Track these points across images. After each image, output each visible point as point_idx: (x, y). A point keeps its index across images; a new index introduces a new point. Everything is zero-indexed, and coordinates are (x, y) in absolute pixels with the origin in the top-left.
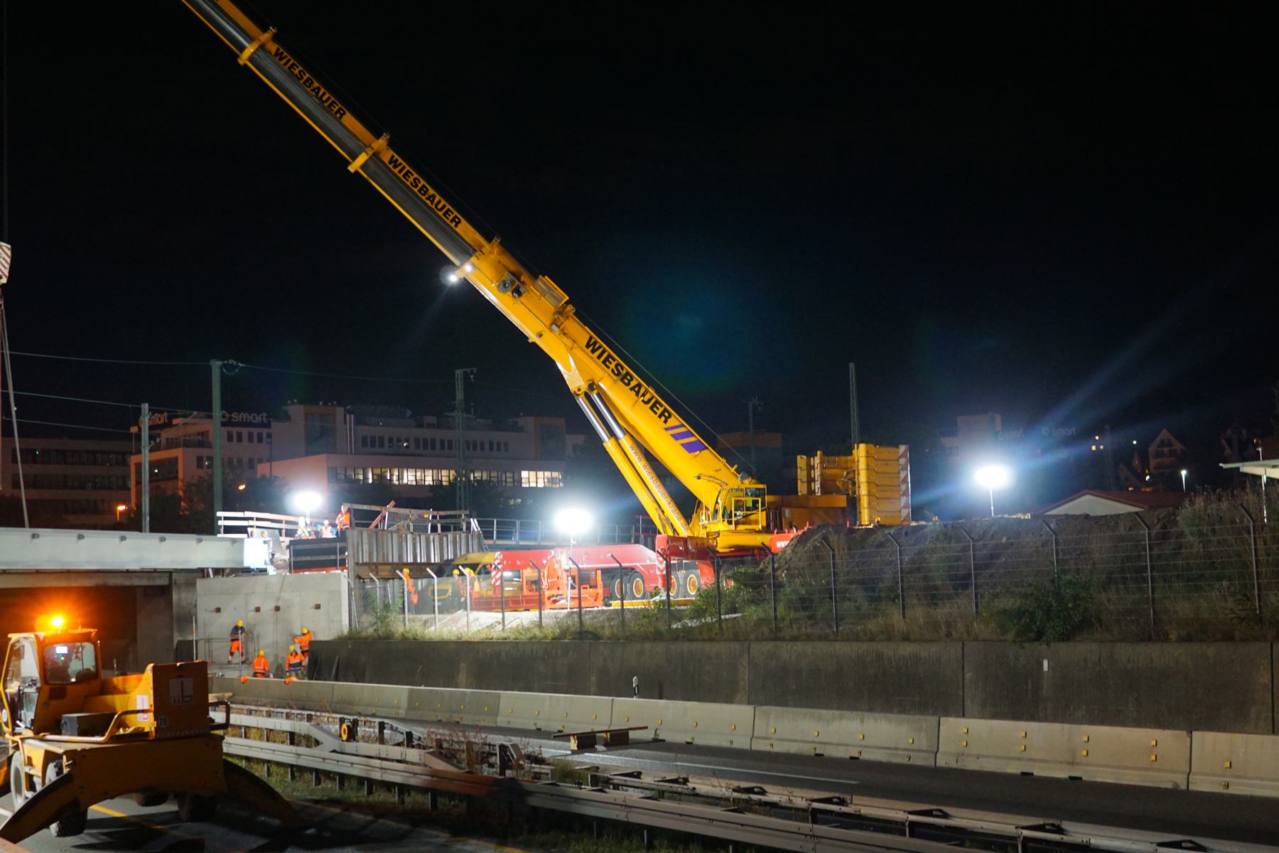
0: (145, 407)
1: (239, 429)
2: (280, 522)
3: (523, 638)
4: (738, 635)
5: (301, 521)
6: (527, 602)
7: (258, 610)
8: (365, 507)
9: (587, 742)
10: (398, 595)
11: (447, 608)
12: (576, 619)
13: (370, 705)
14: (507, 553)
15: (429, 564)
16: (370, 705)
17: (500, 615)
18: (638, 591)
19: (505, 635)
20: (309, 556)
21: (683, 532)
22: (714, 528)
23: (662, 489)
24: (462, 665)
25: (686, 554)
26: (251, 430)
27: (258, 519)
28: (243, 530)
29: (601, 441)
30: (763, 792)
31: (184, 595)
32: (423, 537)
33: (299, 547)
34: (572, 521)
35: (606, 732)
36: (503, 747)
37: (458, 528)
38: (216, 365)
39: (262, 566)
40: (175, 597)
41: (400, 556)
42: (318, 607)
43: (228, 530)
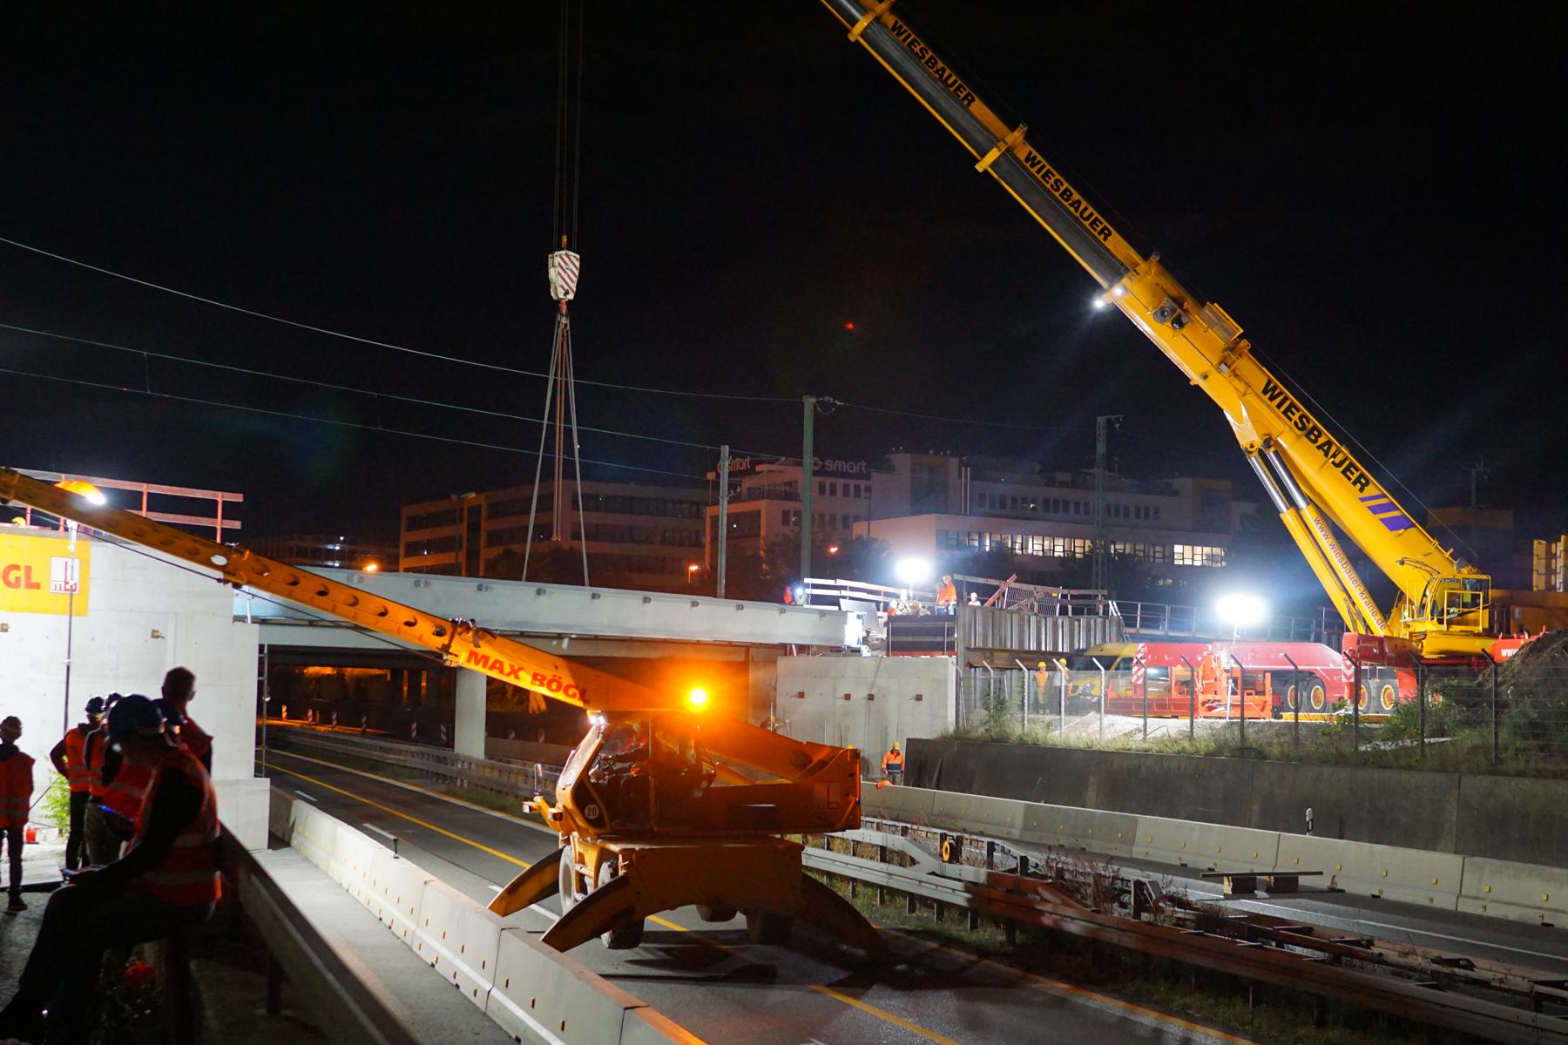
0: (725, 449)
1: (833, 480)
3: (1169, 751)
4: (1445, 764)
5: (903, 594)
6: (1177, 706)
7: (848, 697)
8: (981, 581)
9: (1244, 885)
10: (1016, 689)
13: (977, 821)
14: (1153, 645)
16: (977, 821)
17: (1141, 721)
19: (1146, 746)
20: (911, 637)
21: (1379, 631)
22: (1419, 627)
23: (1354, 575)
24: (1092, 779)
25: (1381, 658)
26: (847, 481)
27: (852, 589)
28: (835, 601)
29: (1277, 511)
30: (1470, 966)
32: (1050, 620)
33: (898, 624)
34: (1238, 611)
35: (1269, 874)
36: (1139, 884)
37: (1092, 611)
38: (809, 402)
39: (854, 645)
41: (1021, 642)
42: (919, 698)
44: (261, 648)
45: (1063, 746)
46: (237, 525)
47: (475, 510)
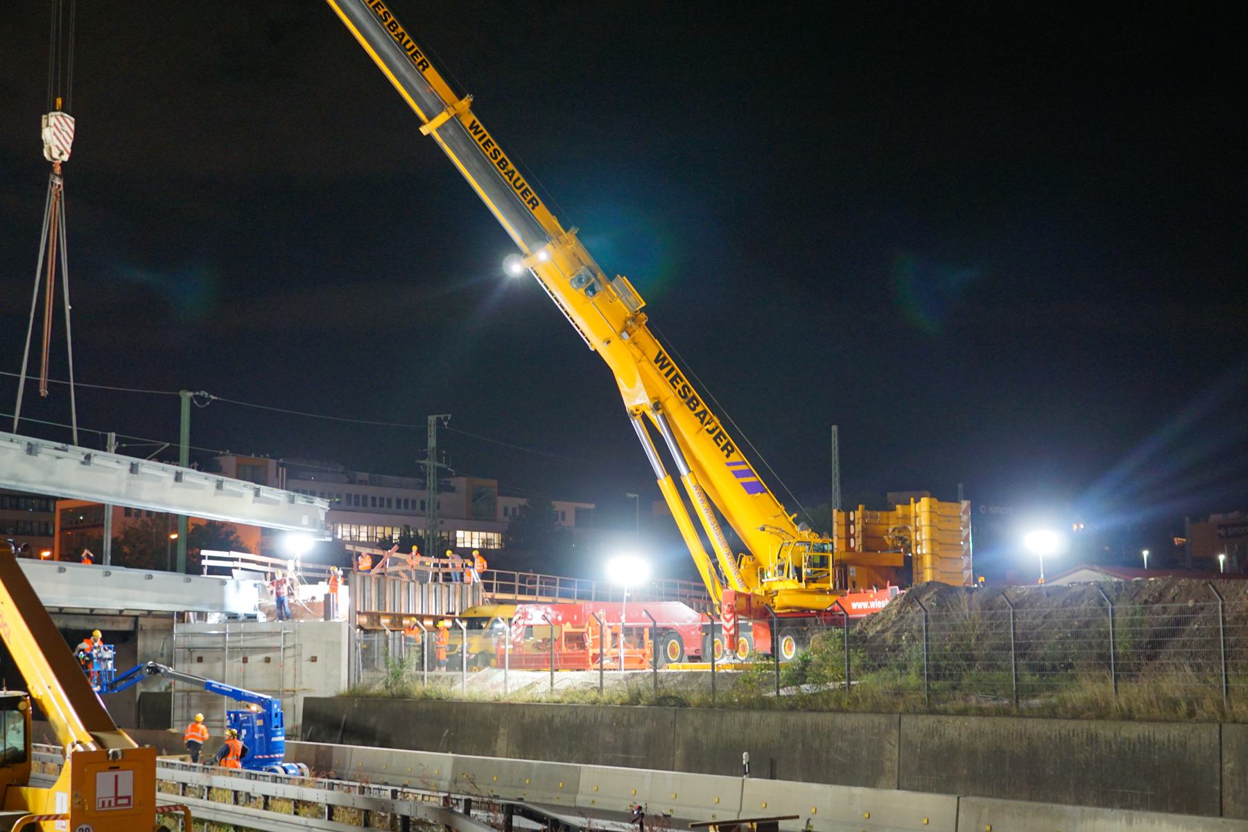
2: (266, 564)
5: (290, 565)
6: (566, 661)
11: (474, 664)
12: (651, 682)
13: (400, 775)
16: (400, 775)
18: (673, 650)
19: (557, 697)
23: (722, 537)
24: (502, 730)
27: (243, 560)
31: (149, 642)
32: (425, 586)
35: (752, 821)
38: (186, 396)
39: (252, 612)
40: (140, 644)
42: (314, 659)
43: (212, 570)
45: (470, 700)
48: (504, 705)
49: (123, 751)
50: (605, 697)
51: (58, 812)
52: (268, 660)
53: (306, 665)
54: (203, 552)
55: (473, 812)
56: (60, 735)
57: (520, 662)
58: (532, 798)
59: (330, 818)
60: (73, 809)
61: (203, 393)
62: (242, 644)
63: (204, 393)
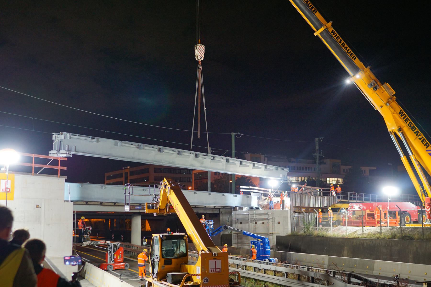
5: (270, 191)
10: (307, 219)
12: (399, 231)
15: (314, 208)
19: (365, 236)
24: (345, 248)
27: (254, 189)
28: (249, 193)
31: (224, 217)
32: (316, 197)
38: (233, 134)
39: (257, 207)
40: (221, 218)
42: (279, 223)
43: (244, 193)
44: (74, 211)
45: (334, 237)
46: (65, 168)
47: (126, 173)
48: (346, 238)
49: (217, 253)
50: (383, 236)
51: (197, 273)
52: (263, 223)
53: (277, 225)
54: (241, 187)
55: (336, 276)
56: (197, 248)
57: (351, 223)
58: (357, 271)
59: (287, 277)
60: (202, 272)
61: (239, 133)
62: (255, 218)
63: (239, 133)
